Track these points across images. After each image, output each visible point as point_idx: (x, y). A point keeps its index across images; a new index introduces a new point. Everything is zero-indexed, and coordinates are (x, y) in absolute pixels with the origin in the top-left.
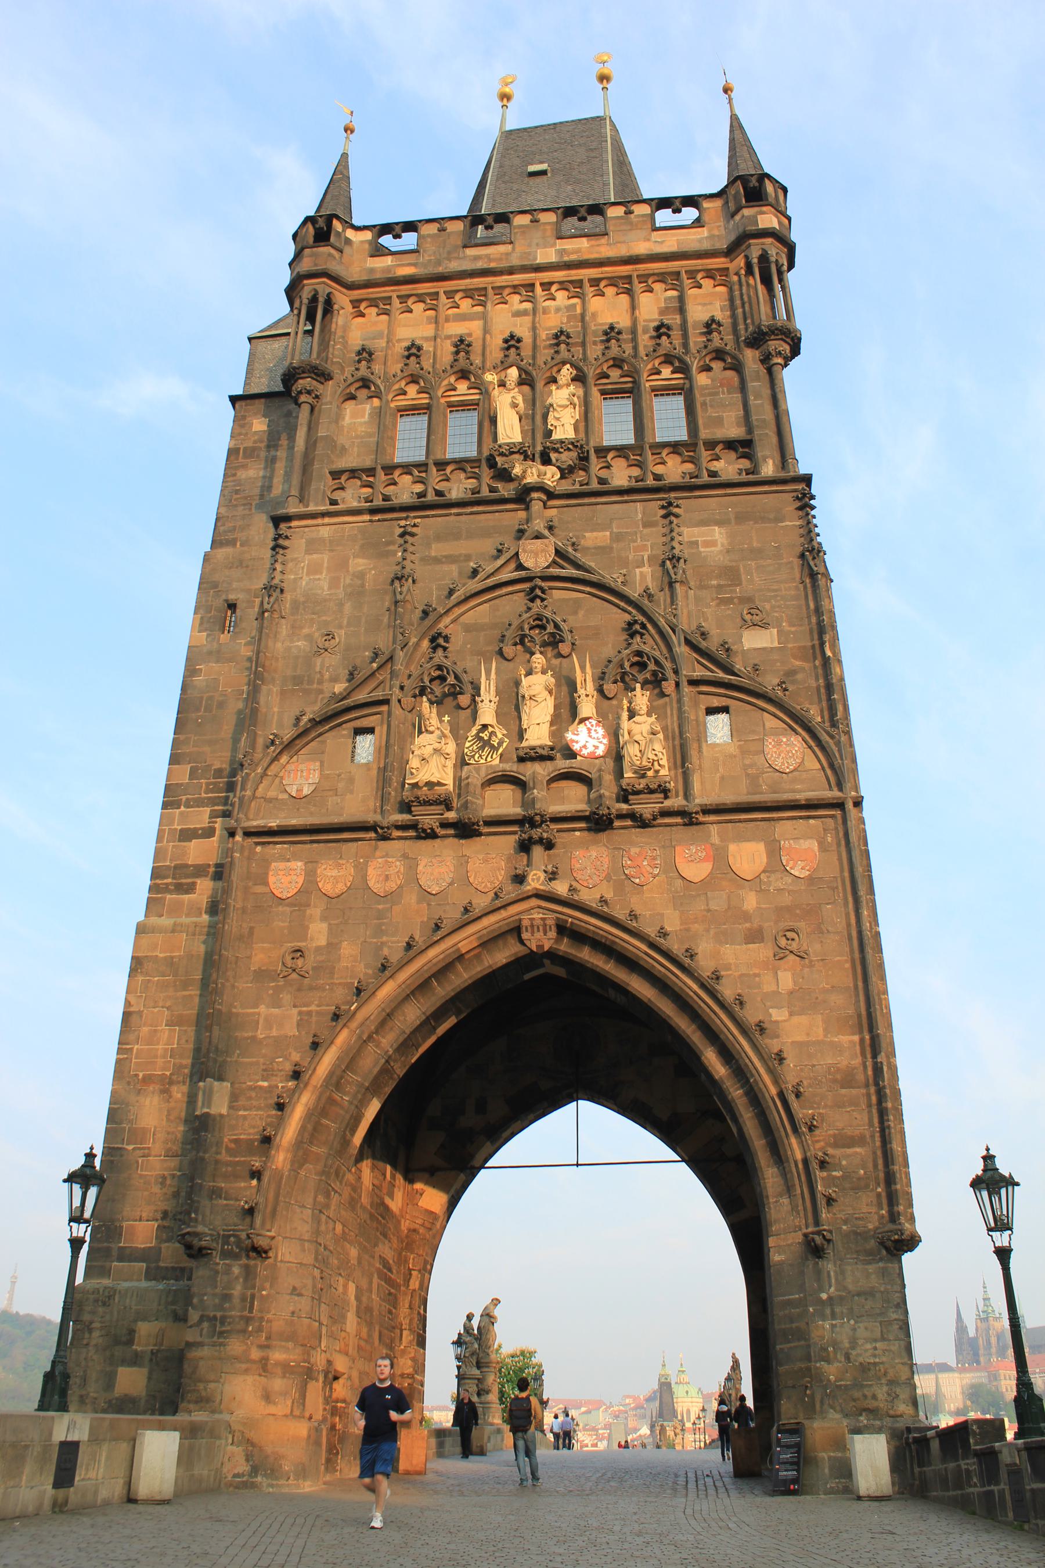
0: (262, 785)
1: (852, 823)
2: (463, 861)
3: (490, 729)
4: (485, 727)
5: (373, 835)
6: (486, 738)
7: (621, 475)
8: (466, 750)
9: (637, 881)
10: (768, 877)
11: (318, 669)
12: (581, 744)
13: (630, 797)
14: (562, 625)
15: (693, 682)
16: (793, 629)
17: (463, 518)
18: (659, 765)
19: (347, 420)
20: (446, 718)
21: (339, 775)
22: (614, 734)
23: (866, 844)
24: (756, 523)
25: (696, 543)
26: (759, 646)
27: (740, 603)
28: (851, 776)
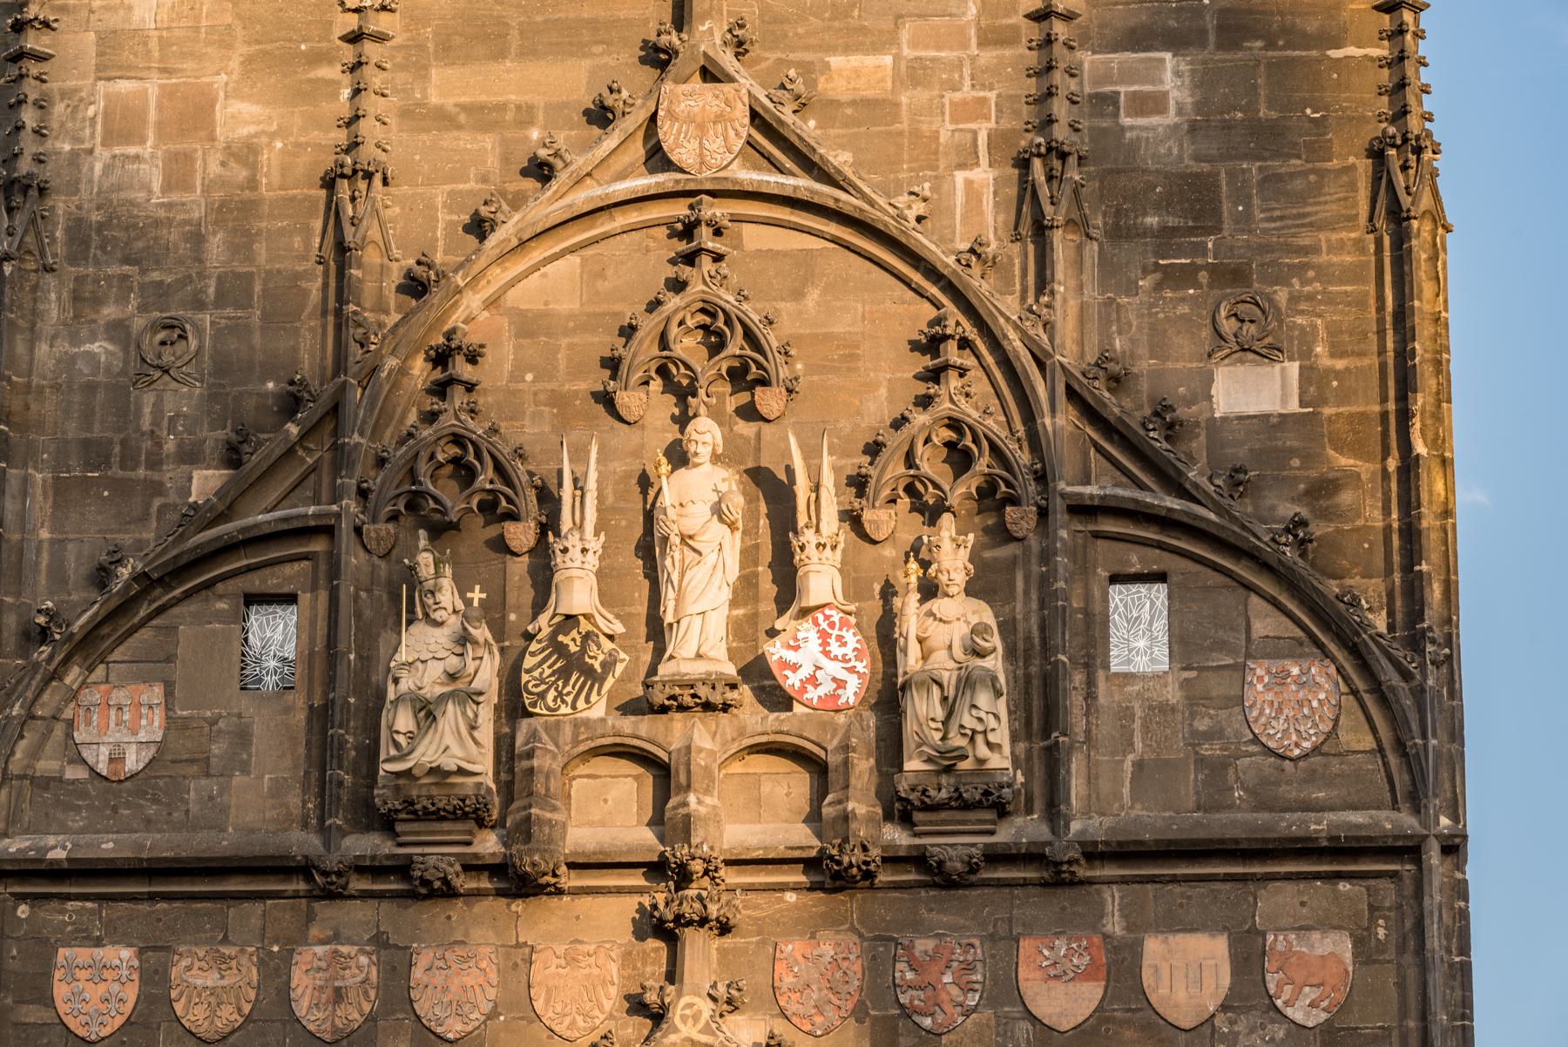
0: (23, 744)
1: (1435, 897)
3: (585, 626)
5: (302, 886)
6: (573, 648)
8: (525, 677)
10: (1232, 1023)
12: (804, 672)
13: (918, 816)
14: (761, 331)
15: (1081, 510)
16: (1340, 364)
18: (988, 744)
20: (477, 595)
21: (213, 722)
23: (1465, 949)
25: (1113, 99)
26: (1252, 410)
28: (1445, 775)
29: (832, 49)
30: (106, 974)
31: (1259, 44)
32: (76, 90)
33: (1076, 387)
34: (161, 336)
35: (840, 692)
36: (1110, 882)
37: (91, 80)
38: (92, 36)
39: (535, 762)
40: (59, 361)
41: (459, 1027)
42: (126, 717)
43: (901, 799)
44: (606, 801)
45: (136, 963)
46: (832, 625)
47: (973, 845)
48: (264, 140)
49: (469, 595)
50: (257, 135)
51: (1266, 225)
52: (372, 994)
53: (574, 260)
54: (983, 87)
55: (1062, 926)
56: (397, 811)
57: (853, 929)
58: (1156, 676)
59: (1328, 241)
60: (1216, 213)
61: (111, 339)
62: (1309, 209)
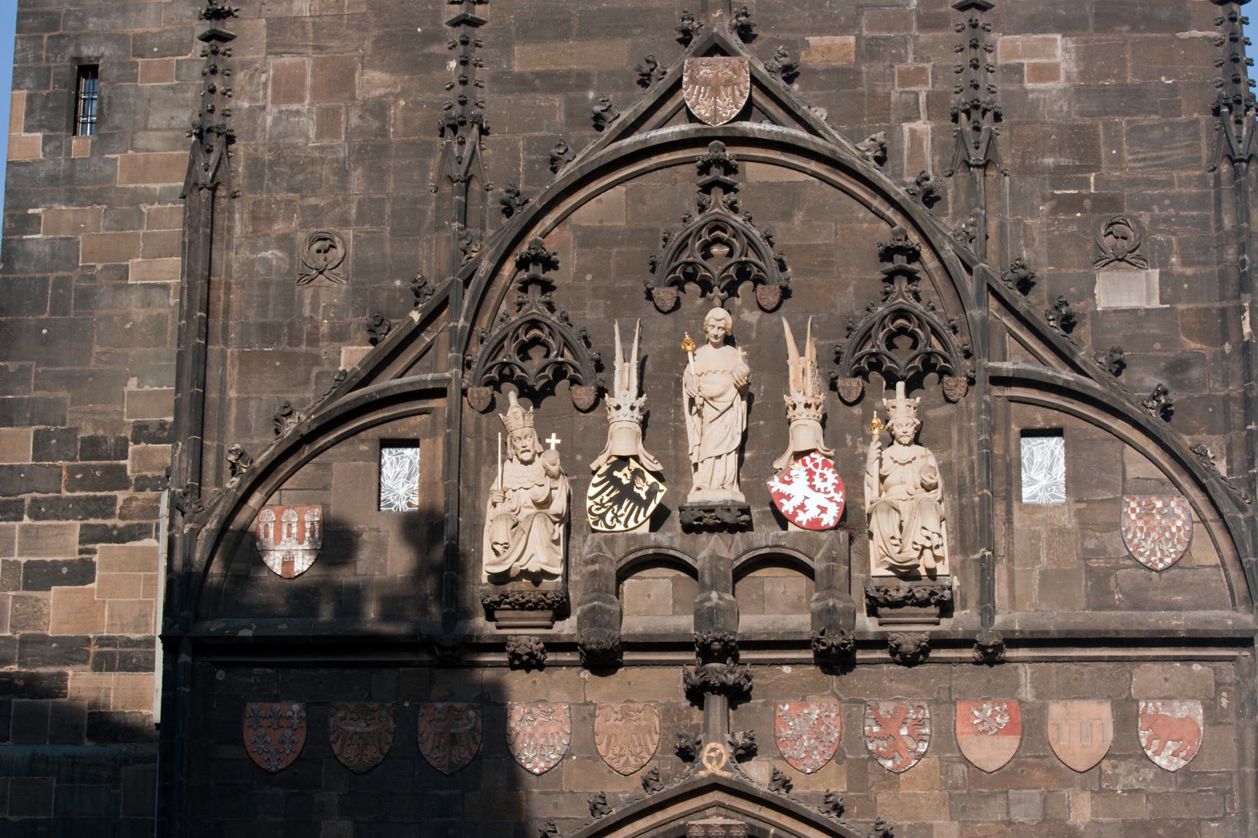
2: (584, 715)
3: (633, 464)
4: (623, 461)
5: (425, 658)
6: (625, 481)
8: (589, 503)
9: (889, 764)
10: (1115, 767)
11: (307, 312)
12: (796, 501)
16: (1189, 271)
20: (553, 441)
22: (851, 476)
24: (1135, 29)
25: (1018, 69)
26: (1125, 304)
27: (1093, 210)
30: (283, 723)
31: (1126, 28)
32: (253, 62)
33: (995, 287)
34: (316, 246)
35: (822, 516)
36: (1024, 661)
37: (262, 56)
38: (264, 22)
40: (242, 265)
41: (542, 765)
42: (294, 530)
44: (649, 596)
45: (304, 714)
46: (816, 466)
47: (923, 632)
48: (391, 99)
49: (548, 441)
50: (386, 95)
51: (1133, 165)
52: (479, 739)
53: (621, 189)
54: (922, 60)
55: (989, 693)
56: (495, 603)
57: (834, 694)
58: (1056, 506)
59: (1179, 177)
60: (1096, 156)
61: (280, 248)
62: (1163, 153)
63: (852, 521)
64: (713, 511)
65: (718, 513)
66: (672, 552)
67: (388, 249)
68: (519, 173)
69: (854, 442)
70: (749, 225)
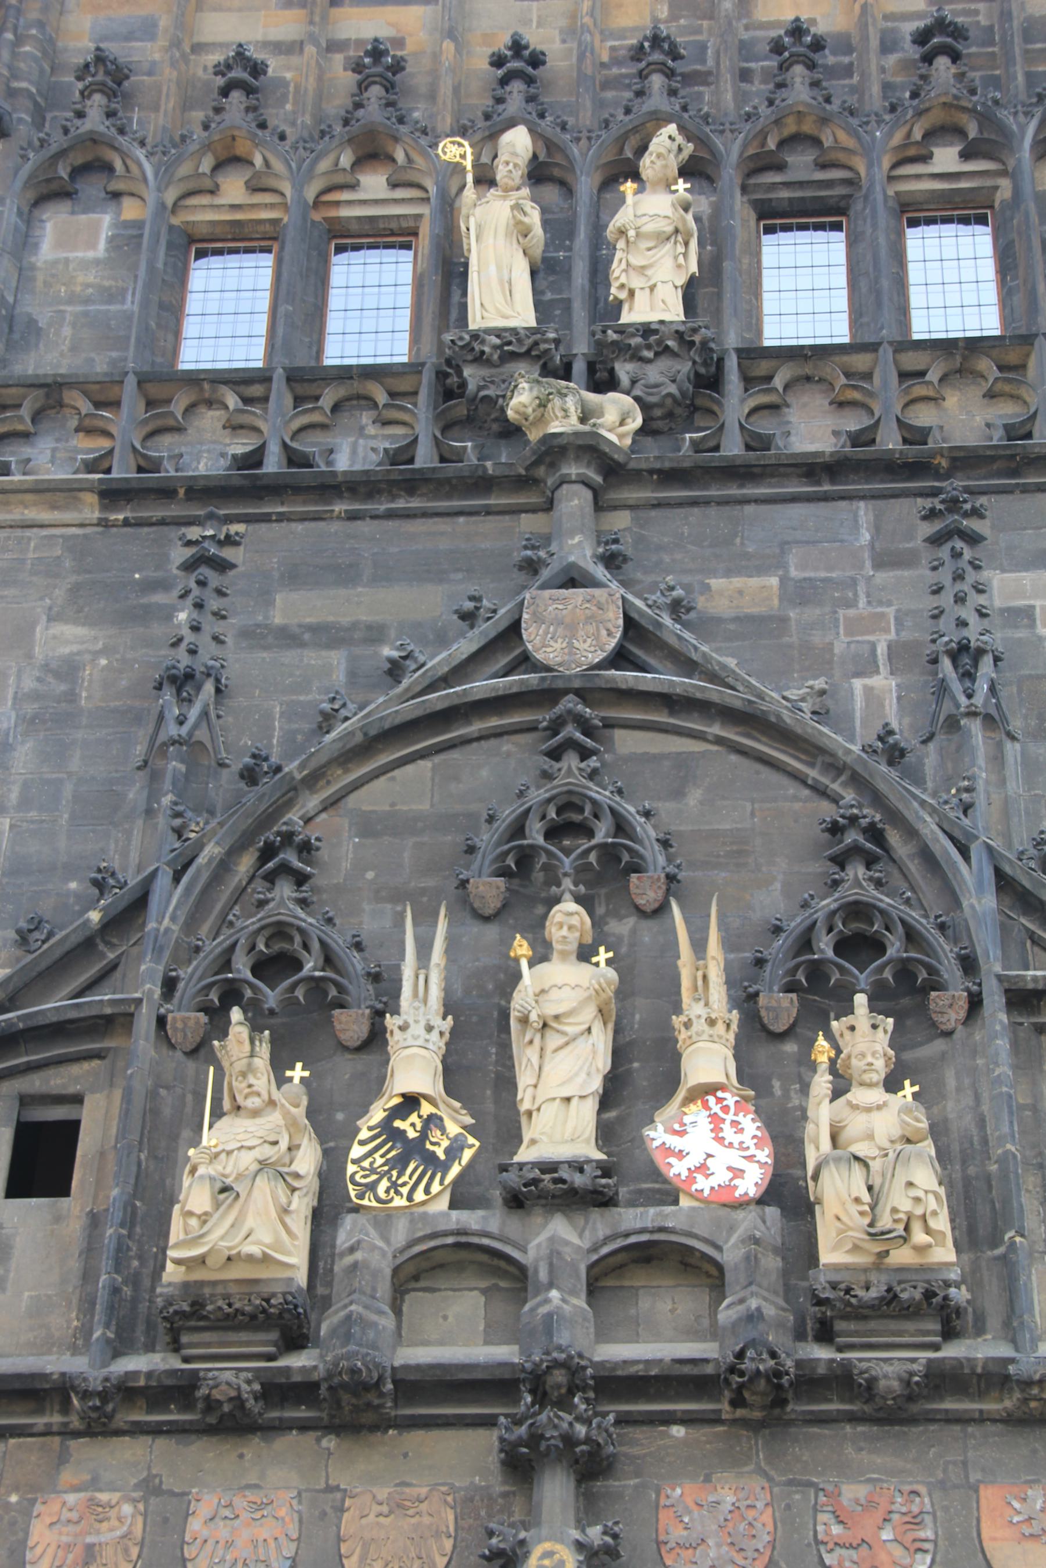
2: (326, 1506)
3: (426, 1109)
4: (411, 1102)
5: (56, 1419)
6: (412, 1134)
7: (812, 429)
8: (351, 1168)
13: (840, 1326)
15: (1022, 999)
17: (364, 527)
18: (928, 1231)
19: (47, 251)
20: (298, 1072)
22: (785, 1134)
29: (713, 573)
33: (1007, 869)
35: (736, 1182)
39: (358, 1256)
43: (820, 1302)
44: (445, 1318)
46: (726, 1109)
47: (913, 1360)
50: (79, 653)
52: (135, 1551)
53: (425, 765)
54: (880, 603)
56: (182, 1315)
63: (789, 1194)
64: (555, 1170)
65: (564, 1173)
66: (485, 1241)
67: (62, 843)
68: (270, 746)
69: (786, 1091)
70: (618, 798)
